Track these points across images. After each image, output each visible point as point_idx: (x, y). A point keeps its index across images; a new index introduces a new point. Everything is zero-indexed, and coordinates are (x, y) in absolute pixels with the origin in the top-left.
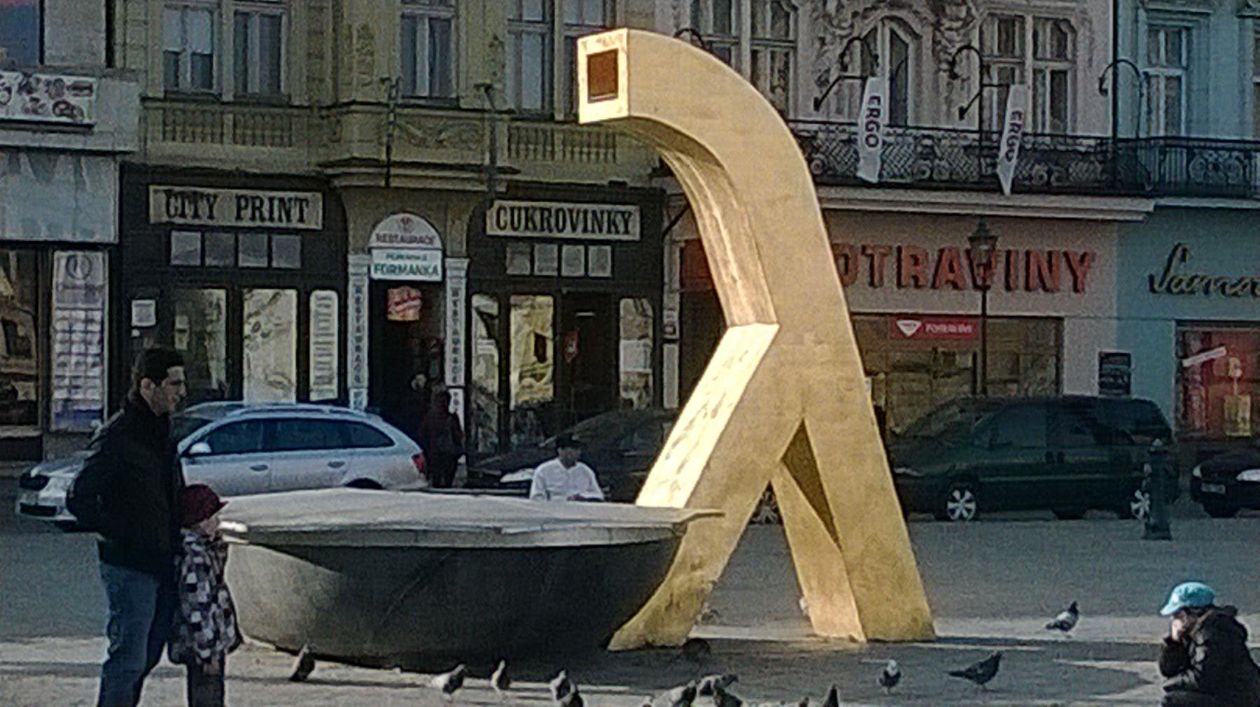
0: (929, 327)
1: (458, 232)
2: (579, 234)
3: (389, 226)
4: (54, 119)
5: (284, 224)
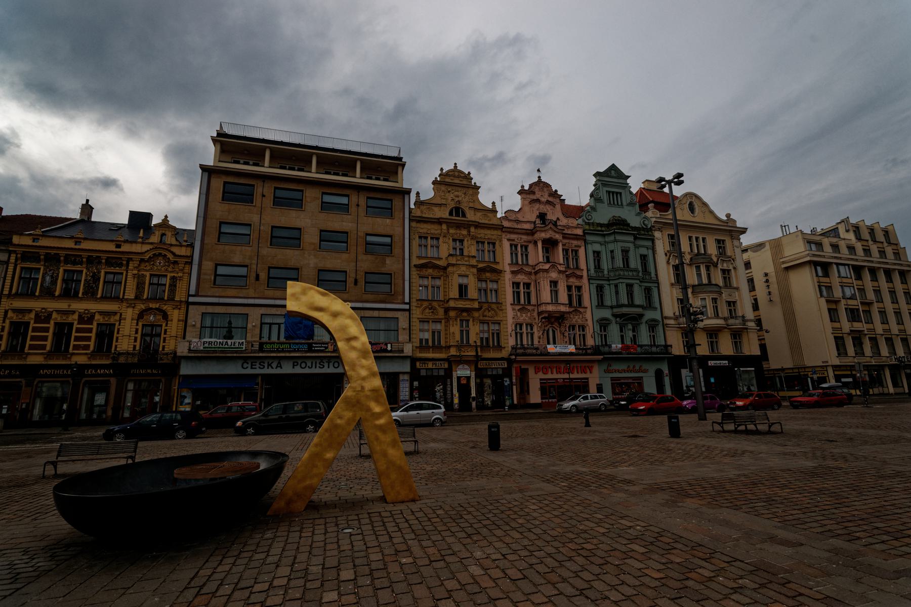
1: (473, 368)
3: (461, 366)
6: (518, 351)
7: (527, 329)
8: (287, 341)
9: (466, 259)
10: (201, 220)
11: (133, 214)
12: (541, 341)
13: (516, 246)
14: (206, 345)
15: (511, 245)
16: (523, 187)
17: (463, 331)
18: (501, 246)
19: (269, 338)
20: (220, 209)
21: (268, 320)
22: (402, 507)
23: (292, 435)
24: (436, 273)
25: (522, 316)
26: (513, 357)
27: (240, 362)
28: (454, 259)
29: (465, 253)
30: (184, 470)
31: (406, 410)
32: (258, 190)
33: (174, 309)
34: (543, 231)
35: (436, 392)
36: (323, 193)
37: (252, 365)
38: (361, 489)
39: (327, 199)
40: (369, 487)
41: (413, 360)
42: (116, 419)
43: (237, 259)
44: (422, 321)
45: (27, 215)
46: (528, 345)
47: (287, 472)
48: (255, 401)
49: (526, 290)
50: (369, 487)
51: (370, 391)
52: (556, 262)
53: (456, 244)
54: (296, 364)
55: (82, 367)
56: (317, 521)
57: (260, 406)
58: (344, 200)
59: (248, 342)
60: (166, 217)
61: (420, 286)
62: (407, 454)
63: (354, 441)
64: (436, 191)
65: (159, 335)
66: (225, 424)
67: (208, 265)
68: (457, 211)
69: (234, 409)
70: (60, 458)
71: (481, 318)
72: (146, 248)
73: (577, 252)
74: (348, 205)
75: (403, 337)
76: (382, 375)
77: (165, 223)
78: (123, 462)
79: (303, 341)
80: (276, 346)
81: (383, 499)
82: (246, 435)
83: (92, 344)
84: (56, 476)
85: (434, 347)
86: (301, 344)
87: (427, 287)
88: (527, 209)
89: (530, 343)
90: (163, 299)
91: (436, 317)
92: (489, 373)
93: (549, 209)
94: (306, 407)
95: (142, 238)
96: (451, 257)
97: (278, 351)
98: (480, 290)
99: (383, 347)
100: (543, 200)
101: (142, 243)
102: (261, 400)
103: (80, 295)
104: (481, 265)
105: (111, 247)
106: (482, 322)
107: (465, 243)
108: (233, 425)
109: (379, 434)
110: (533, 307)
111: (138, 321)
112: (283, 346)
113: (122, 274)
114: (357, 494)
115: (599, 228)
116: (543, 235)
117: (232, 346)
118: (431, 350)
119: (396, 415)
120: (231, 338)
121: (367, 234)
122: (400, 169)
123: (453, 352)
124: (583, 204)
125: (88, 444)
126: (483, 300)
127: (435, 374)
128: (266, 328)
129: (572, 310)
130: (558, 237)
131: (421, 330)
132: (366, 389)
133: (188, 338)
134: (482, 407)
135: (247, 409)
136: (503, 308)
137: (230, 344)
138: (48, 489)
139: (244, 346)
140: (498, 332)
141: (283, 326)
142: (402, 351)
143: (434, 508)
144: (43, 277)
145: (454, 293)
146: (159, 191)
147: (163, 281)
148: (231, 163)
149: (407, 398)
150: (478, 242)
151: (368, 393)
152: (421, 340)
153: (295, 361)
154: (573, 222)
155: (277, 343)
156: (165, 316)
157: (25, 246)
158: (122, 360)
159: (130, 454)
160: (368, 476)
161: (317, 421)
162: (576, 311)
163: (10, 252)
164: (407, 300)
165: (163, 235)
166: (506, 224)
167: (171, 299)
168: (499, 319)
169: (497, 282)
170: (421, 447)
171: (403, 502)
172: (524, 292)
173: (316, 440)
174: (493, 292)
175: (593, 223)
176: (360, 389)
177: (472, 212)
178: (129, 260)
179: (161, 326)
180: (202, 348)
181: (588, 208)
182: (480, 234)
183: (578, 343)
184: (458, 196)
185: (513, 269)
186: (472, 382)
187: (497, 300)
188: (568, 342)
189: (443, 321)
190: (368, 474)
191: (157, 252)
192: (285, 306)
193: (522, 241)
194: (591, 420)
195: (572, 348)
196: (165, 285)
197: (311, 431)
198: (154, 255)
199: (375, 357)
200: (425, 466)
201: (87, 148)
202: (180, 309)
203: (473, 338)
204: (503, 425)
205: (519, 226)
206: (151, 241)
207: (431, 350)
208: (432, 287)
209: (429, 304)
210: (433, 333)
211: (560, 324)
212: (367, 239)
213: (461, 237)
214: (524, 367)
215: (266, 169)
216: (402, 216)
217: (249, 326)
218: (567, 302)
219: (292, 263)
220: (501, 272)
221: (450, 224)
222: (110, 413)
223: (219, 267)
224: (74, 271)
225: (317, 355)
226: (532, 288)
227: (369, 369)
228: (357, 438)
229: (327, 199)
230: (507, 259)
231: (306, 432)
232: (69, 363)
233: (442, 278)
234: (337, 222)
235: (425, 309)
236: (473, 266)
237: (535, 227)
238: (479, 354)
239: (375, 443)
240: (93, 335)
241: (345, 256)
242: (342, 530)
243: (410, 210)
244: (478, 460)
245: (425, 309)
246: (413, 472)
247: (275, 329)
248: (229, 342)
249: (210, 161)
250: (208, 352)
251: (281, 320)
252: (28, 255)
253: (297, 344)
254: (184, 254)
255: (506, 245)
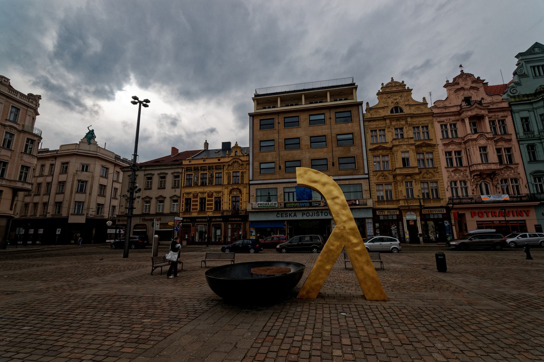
1: (418, 214)
2: (436, 213)
3: (408, 213)
6: (455, 201)
7: (461, 185)
8: (298, 202)
9: (406, 140)
10: (251, 141)
11: (223, 143)
12: (475, 192)
13: (446, 126)
14: (259, 205)
15: (441, 126)
16: (448, 81)
17: (408, 189)
18: (433, 127)
19: (289, 201)
20: (260, 135)
21: (287, 190)
22: (377, 304)
23: (305, 254)
24: (384, 153)
25: (456, 175)
26: (451, 205)
27: (276, 214)
28: (397, 141)
29: (405, 136)
30: (256, 269)
31: (372, 241)
32: (276, 121)
33: (244, 188)
34: (468, 111)
35: (392, 230)
36: (310, 115)
37: (281, 215)
38: (349, 289)
39: (312, 118)
40: (353, 288)
41: (374, 210)
42: (225, 242)
43: (269, 159)
44: (378, 185)
45: (187, 152)
46: (463, 196)
47: (305, 275)
48: (285, 235)
49: (457, 156)
50: (353, 288)
51: (349, 229)
52: (484, 132)
53: (397, 131)
54: (304, 214)
55: (211, 218)
56: (325, 306)
57: (288, 238)
58: (322, 117)
59: (278, 203)
60: (237, 142)
61: (374, 162)
62: (377, 269)
63: (341, 260)
64: (380, 99)
65: (239, 201)
66: (271, 246)
67: (257, 164)
68: (397, 109)
69: (275, 239)
70: (207, 259)
71: (422, 179)
72: (230, 159)
73: (503, 121)
74: (324, 119)
75: (366, 195)
76: (356, 219)
77: (236, 146)
78: (230, 263)
79: (307, 201)
80: (292, 204)
81: (363, 297)
82: (282, 253)
83: (213, 206)
84: (206, 267)
85: (387, 201)
86: (306, 202)
87: (379, 162)
88: (453, 97)
89: (465, 195)
90: (239, 183)
91: (388, 181)
92: (432, 217)
93: (473, 93)
94: (311, 238)
95: (228, 154)
96: (395, 141)
97: (294, 207)
98: (419, 160)
99: (354, 202)
100: (466, 87)
101: (228, 157)
102: (288, 234)
103: (207, 185)
104: (418, 143)
105: (216, 161)
106: (423, 182)
107: (405, 130)
108: (275, 247)
109: (357, 256)
110: (465, 168)
111: (230, 194)
112: (296, 204)
113: (222, 173)
114: (346, 292)
115: (526, 98)
116: (470, 113)
117: (271, 205)
118: (386, 202)
119: (367, 244)
120: (270, 201)
121: (337, 135)
122: (354, 90)
123: (402, 203)
124: (507, 82)
125: (216, 254)
126: (422, 166)
127: (390, 218)
128: (287, 195)
129: (502, 167)
130: (483, 112)
131: (377, 191)
132: (347, 228)
133: (251, 202)
134: (427, 240)
135: (281, 239)
136: (439, 171)
137: (270, 204)
138: (203, 272)
139: (277, 205)
140: (436, 188)
141: (295, 194)
142: (366, 204)
143: (400, 308)
144: (194, 178)
145: (399, 164)
146: (232, 130)
147: (238, 174)
148: (262, 109)
149: (372, 234)
150: (414, 128)
151: (348, 231)
152: (378, 197)
153: (303, 212)
154: (498, 98)
155: (293, 203)
156: (240, 192)
157: (187, 165)
158: (225, 214)
159: (232, 259)
160: (352, 282)
161: (318, 246)
162: (507, 167)
163: (182, 168)
164: (366, 172)
165: (236, 152)
166: (435, 111)
167: (242, 183)
168: (436, 179)
169: (432, 153)
170: (385, 266)
171: (377, 301)
172: (456, 158)
173: (319, 257)
174: (430, 161)
175: (518, 95)
176: (343, 228)
177: (408, 108)
178: (224, 166)
179: (239, 197)
180: (257, 207)
181: (512, 84)
182: (415, 122)
183: (511, 192)
184: (396, 99)
185: (445, 142)
186: (418, 223)
187: (433, 166)
188: (501, 192)
189: (393, 184)
190: (352, 281)
191: (234, 161)
192: (296, 182)
193: (451, 121)
194: (532, 254)
195: (506, 197)
196: (239, 176)
197: (315, 252)
198: (233, 162)
199: (351, 209)
200: (390, 279)
201: (203, 116)
202: (246, 188)
203: (416, 193)
204: (449, 255)
205: (447, 111)
206: (231, 155)
207: (386, 202)
208: (382, 162)
209: (382, 173)
210: (386, 191)
211: (492, 179)
212: (338, 138)
213: (401, 126)
214: (461, 212)
215: (279, 109)
216: (358, 120)
217: (278, 194)
218: (498, 161)
219: (297, 158)
220: (434, 146)
221: (391, 119)
222: (223, 239)
223: (261, 164)
224: (204, 174)
225: (314, 208)
226: (463, 154)
227: (347, 216)
228: (343, 257)
229: (312, 118)
230: (439, 135)
231: (312, 252)
232: (205, 216)
233: (389, 155)
234: (319, 130)
235: (379, 176)
236: (412, 145)
237: (461, 109)
238: (422, 204)
239: (356, 262)
240: (213, 203)
241: (325, 150)
242: (340, 313)
243: (363, 115)
244: (429, 278)
245: (379, 176)
246: (382, 282)
247: (291, 194)
248: (270, 203)
249: (253, 110)
250: (260, 209)
251: (294, 190)
252: (188, 169)
253: (304, 203)
254: (245, 160)
255: (437, 126)
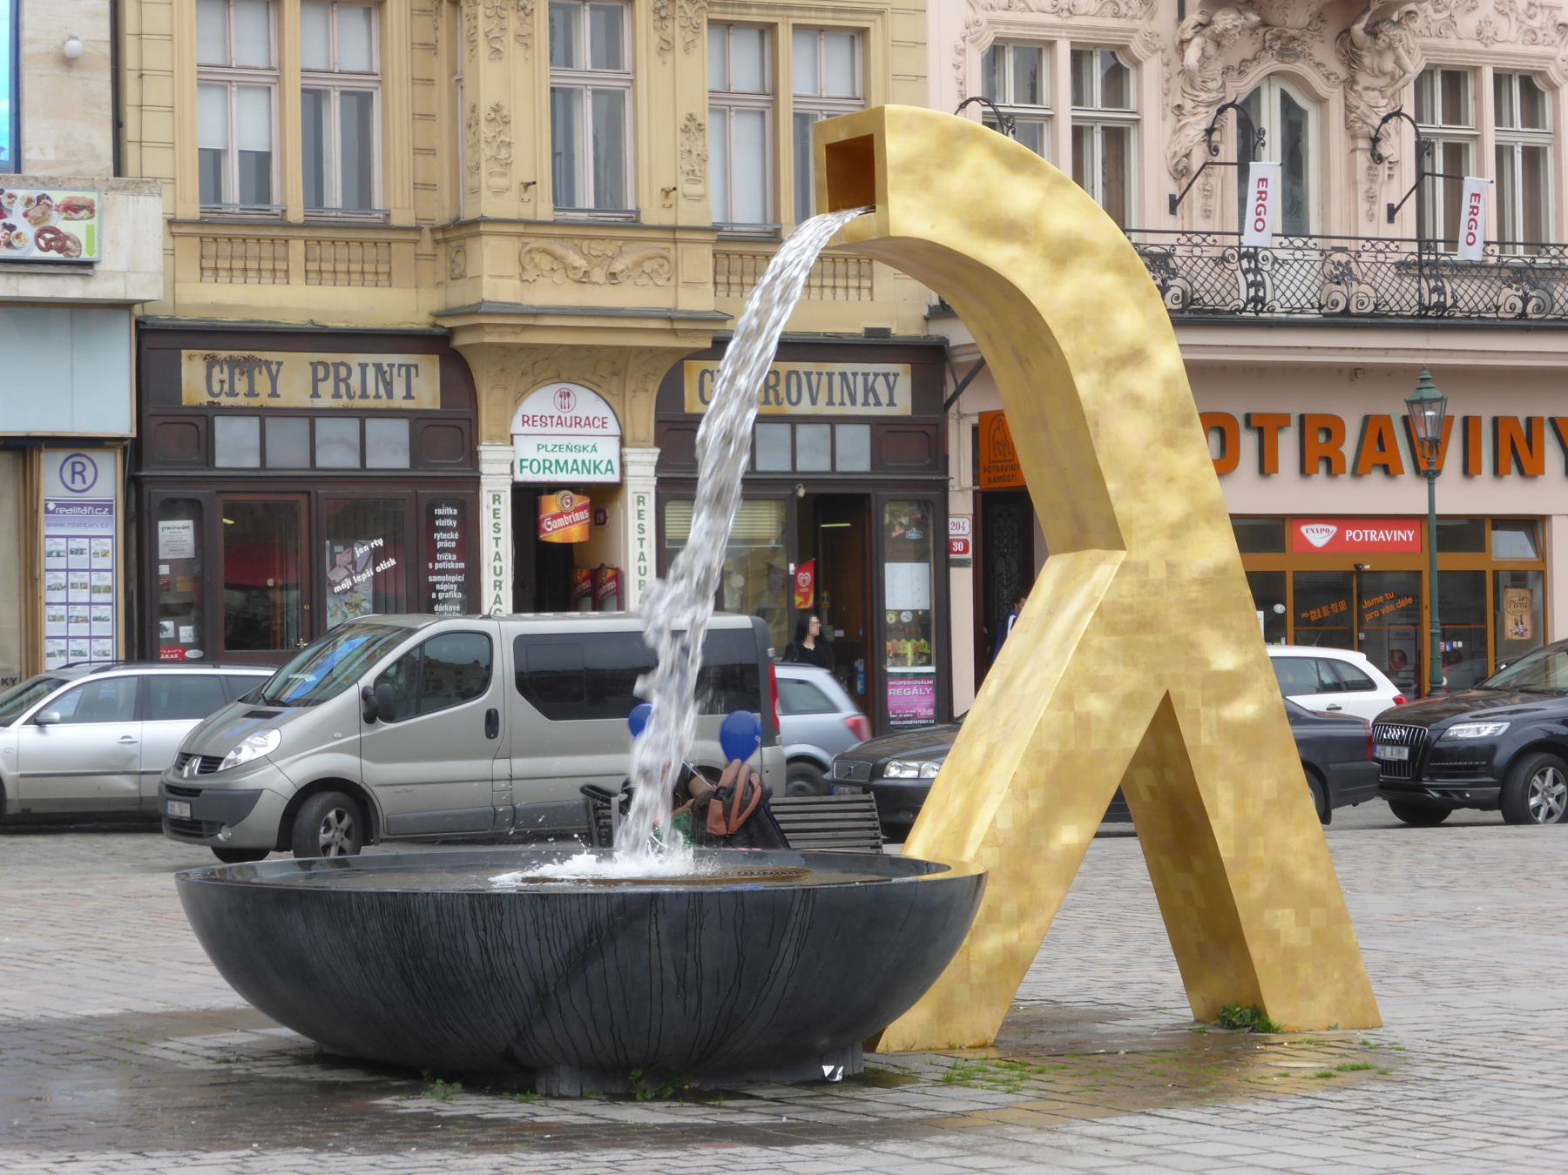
0: (1349, 534)
3: (541, 402)
4: (37, 254)
5: (383, 403)
118: (297, 248)
127: (336, 455)
131: (214, 79)
152: (212, 161)
186: (632, 522)
207: (297, 248)
211: (1351, 58)
